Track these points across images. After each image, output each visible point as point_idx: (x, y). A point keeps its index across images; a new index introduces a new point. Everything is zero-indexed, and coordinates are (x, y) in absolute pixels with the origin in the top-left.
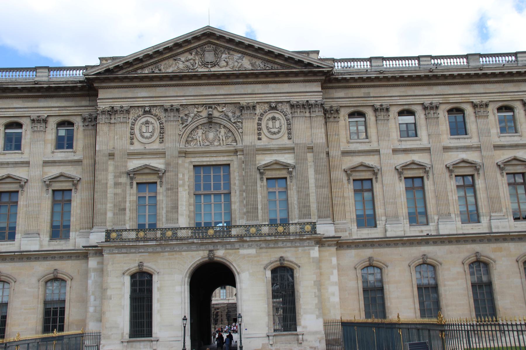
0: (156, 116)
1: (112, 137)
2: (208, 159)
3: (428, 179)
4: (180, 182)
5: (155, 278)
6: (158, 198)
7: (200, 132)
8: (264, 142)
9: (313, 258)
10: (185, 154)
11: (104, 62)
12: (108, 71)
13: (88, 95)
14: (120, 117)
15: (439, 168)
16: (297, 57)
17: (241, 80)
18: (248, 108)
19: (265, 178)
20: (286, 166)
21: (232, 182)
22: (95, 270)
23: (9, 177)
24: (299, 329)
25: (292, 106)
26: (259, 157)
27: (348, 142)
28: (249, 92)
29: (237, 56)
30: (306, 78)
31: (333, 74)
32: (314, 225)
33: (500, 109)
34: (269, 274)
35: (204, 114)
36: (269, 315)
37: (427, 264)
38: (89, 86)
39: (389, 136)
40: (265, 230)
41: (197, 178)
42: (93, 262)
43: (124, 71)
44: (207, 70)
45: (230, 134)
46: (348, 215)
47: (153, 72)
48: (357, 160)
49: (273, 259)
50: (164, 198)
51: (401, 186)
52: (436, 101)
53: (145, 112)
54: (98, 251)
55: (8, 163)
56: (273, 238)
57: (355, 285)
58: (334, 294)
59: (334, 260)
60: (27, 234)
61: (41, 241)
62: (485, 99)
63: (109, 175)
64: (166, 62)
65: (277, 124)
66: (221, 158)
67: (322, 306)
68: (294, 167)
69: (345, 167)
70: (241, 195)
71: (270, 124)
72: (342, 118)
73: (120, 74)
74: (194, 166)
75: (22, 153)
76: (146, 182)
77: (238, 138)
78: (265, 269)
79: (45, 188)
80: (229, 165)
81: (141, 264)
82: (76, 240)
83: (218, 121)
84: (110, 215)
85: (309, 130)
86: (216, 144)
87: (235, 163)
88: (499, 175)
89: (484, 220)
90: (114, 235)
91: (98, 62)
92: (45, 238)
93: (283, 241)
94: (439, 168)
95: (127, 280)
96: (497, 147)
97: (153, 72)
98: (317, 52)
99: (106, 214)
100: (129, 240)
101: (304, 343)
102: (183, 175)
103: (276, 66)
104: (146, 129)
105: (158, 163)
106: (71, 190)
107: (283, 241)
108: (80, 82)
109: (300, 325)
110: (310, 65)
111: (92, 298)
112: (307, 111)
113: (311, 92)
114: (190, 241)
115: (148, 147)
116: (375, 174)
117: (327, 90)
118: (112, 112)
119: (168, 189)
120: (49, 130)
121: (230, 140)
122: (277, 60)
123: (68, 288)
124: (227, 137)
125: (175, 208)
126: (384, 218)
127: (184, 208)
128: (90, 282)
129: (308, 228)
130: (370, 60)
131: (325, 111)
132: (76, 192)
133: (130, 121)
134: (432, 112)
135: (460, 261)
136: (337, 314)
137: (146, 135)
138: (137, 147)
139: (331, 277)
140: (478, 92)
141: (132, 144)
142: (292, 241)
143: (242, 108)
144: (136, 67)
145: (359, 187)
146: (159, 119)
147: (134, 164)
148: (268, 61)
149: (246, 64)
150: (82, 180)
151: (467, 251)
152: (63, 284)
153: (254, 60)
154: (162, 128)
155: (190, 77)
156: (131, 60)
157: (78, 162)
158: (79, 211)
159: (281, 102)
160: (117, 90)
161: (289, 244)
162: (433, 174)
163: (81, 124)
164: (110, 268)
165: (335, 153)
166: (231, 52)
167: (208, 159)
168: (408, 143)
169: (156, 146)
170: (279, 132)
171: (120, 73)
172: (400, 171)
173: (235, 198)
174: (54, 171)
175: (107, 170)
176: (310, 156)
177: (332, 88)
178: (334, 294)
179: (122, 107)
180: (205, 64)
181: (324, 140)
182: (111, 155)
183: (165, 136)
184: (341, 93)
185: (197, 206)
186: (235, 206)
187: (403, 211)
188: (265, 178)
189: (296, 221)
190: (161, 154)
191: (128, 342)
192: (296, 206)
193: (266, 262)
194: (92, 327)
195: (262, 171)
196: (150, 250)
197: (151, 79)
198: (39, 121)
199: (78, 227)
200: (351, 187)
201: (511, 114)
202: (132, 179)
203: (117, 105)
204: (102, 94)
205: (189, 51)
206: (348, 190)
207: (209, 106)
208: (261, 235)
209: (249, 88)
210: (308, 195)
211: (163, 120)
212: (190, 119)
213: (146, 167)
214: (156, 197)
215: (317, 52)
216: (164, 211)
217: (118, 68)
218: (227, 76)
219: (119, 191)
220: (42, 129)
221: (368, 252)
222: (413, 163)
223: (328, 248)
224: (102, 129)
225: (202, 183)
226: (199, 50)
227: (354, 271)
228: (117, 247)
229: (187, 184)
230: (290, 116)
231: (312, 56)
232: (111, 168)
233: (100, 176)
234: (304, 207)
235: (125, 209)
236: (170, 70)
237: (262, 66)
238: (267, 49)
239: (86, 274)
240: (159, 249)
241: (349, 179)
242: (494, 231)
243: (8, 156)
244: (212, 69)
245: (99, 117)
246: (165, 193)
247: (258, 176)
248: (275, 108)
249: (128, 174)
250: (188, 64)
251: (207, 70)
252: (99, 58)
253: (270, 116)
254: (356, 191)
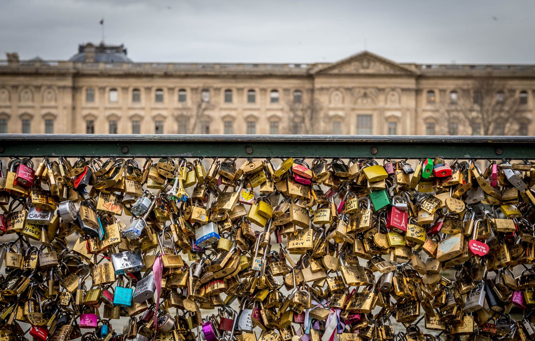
8: (388, 106)
10: (353, 110)
14: (325, 92)
16: (406, 67)
35: (362, 91)
87: (375, 114)
118: (322, 89)
138: (332, 105)
180: (363, 68)
205: (357, 61)
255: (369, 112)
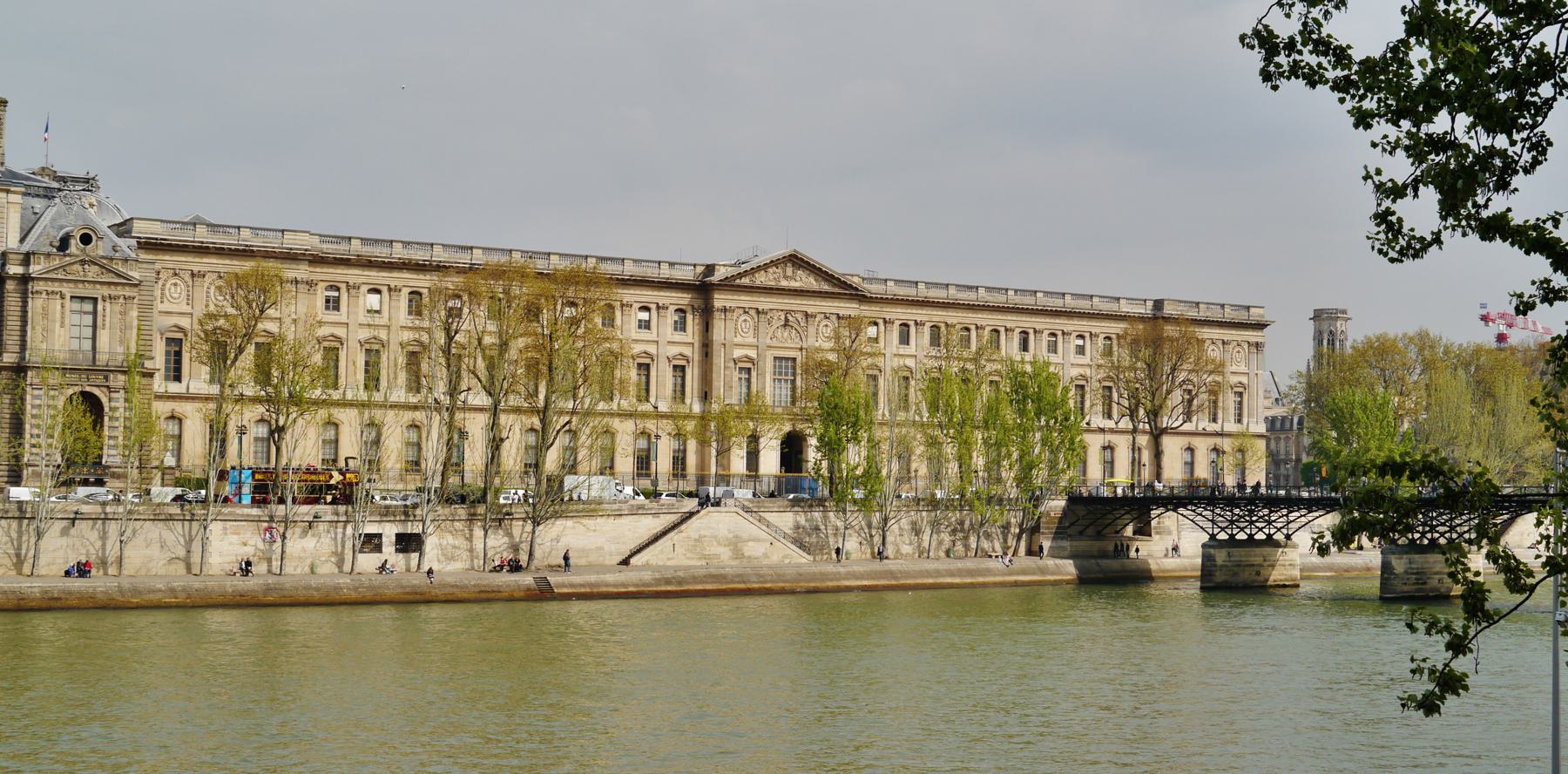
118: (725, 310)
147: (738, 353)
169: (751, 340)
180: (786, 277)
203: (728, 305)
207: (788, 312)
255: (791, 354)
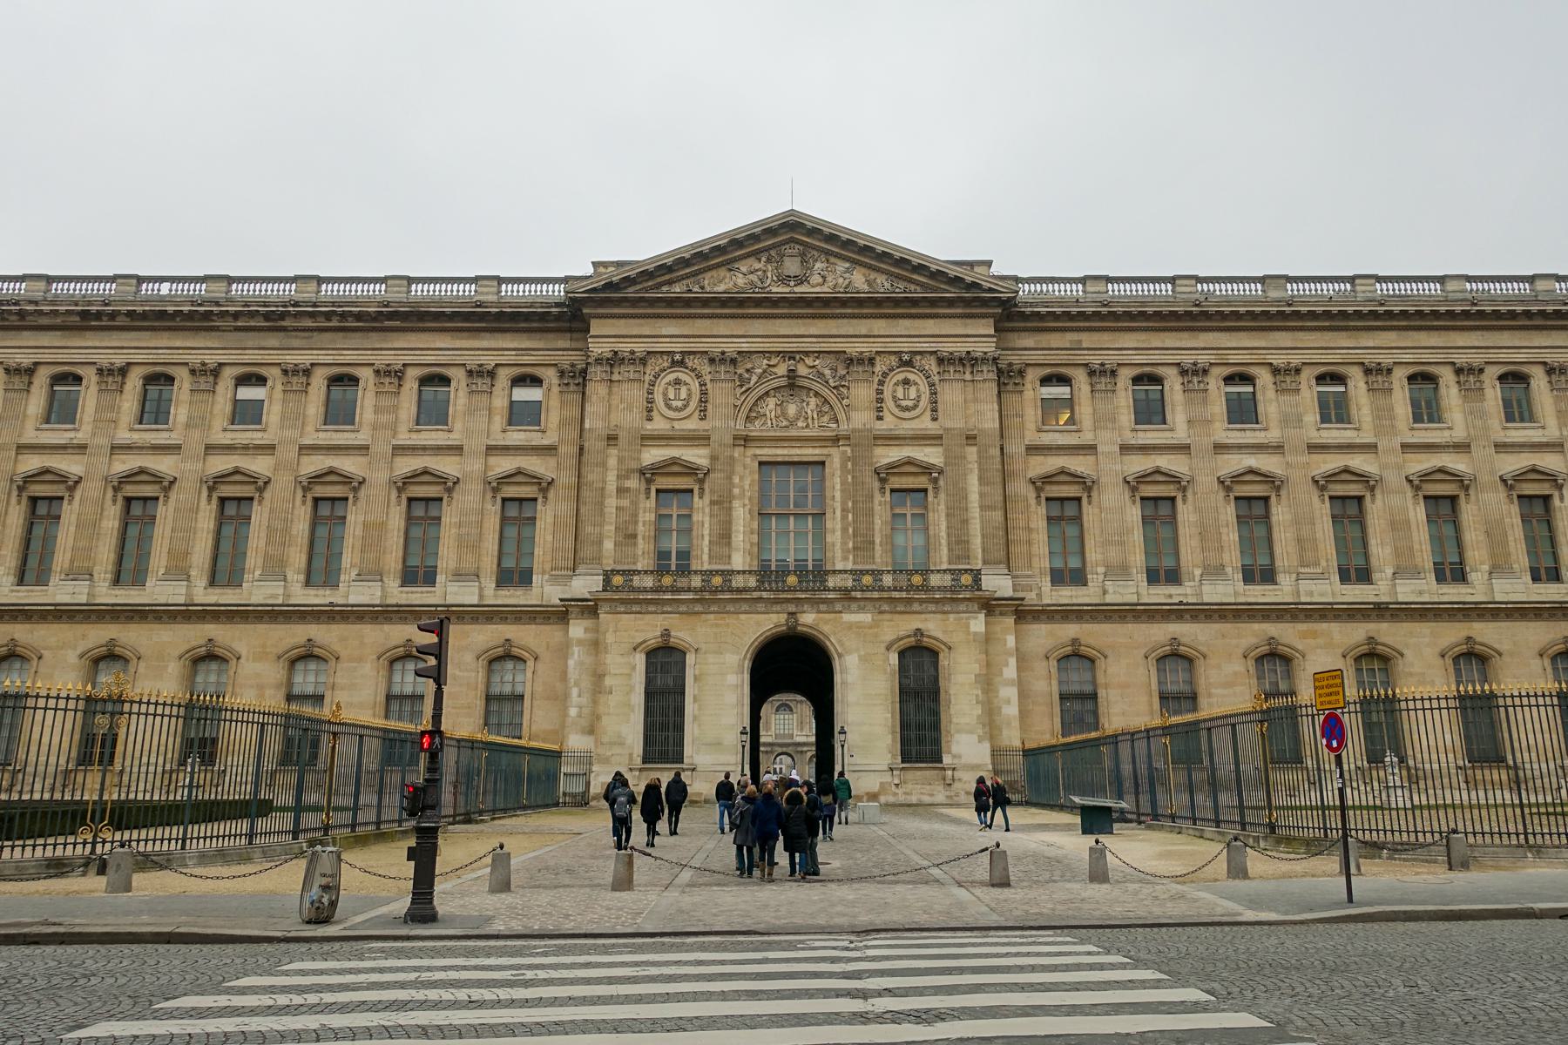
0: (693, 370)
1: (614, 405)
2: (785, 451)
3: (1184, 501)
4: (736, 491)
5: (690, 659)
6: (695, 518)
7: (772, 402)
8: (888, 424)
9: (975, 634)
10: (745, 441)
11: (602, 270)
12: (610, 286)
13: (570, 330)
14: (629, 371)
15: (1206, 483)
16: (953, 272)
17: (849, 311)
18: (860, 361)
19: (888, 488)
20: (926, 469)
21: (828, 494)
22: (580, 642)
23: (425, 472)
24: (947, 759)
25: (941, 361)
26: (879, 451)
27: (1039, 431)
28: (864, 332)
29: (842, 266)
30: (968, 311)
31: (1016, 305)
32: (977, 575)
33: (1321, 379)
34: (894, 659)
35: (782, 370)
36: (893, 732)
37: (1176, 657)
38: (573, 312)
39: (1114, 420)
40: (888, 580)
41: (763, 484)
42: (578, 629)
43: (638, 287)
44: (787, 290)
45: (826, 408)
46: (1035, 561)
47: (690, 291)
48: (1053, 463)
49: (902, 633)
50: (707, 519)
51: (1134, 513)
52: (1203, 359)
53: (674, 363)
54: (589, 608)
55: (424, 448)
56: (904, 595)
57: (1046, 684)
58: (1008, 702)
59: (1011, 641)
60: (459, 575)
61: (481, 589)
62: (1296, 359)
63: (609, 472)
64: (714, 273)
65: (913, 393)
66: (810, 451)
67: (990, 722)
68: (941, 472)
69: (1031, 474)
70: (844, 517)
71: (900, 393)
72: (1028, 386)
73: (631, 293)
74: (761, 463)
75: (450, 431)
76: (672, 485)
77: (841, 416)
78: (888, 649)
79: (489, 495)
80: (823, 463)
81: (666, 634)
82: (545, 591)
83: (806, 383)
84: (609, 545)
85: (970, 405)
86: (800, 424)
87: (835, 457)
88: (1316, 499)
89: (1285, 581)
90: (618, 580)
91: (590, 271)
92: (490, 584)
93: (921, 601)
94: (1206, 483)
95: (640, 660)
96: (1314, 448)
97: (690, 291)
98: (989, 264)
99: (601, 543)
100: (645, 590)
101: (956, 785)
102: (741, 478)
103: (913, 287)
104: (676, 393)
105: (697, 456)
106: (535, 500)
107: (921, 601)
108: (557, 305)
109: (949, 752)
110: (975, 286)
111: (575, 691)
112: (968, 370)
113: (977, 336)
114: (756, 595)
115: (677, 425)
116: (1089, 490)
117: (1003, 335)
118: (615, 360)
119: (712, 503)
120: (497, 390)
121: (826, 419)
122: (915, 277)
123: (529, 674)
124: (821, 413)
125: (724, 537)
126: (1101, 570)
127: (741, 537)
128: (571, 663)
129: (966, 579)
130: (1083, 280)
131: (1000, 372)
132: (545, 503)
133: (647, 378)
134: (1195, 380)
135: (1240, 652)
136: (1012, 738)
137: (674, 404)
138: (658, 425)
139: (1005, 670)
140: (1282, 346)
141: (650, 419)
142: (937, 601)
143: (850, 361)
144: (659, 280)
145: (1056, 513)
146: (698, 377)
148: (898, 277)
149: (859, 280)
150: (557, 483)
151: (1254, 634)
152: (520, 666)
153: (873, 275)
154: (704, 393)
155: (759, 303)
156: (651, 267)
157: (550, 450)
158: (549, 538)
159: (920, 353)
160: (623, 321)
161: (932, 607)
162: (1195, 494)
163: (555, 381)
164: (610, 638)
165: (1016, 448)
166: (832, 260)
167: (785, 451)
168: (1149, 435)
169: (692, 425)
170: (915, 406)
171: (631, 289)
172: (1134, 485)
173: (834, 523)
174: (505, 465)
175: (604, 465)
176: (972, 453)
177: (1013, 330)
178: (1008, 702)
179: (632, 353)
180: (784, 280)
181: (997, 425)
182: (612, 439)
183: (710, 407)
184: (1028, 341)
185: (763, 534)
186: (835, 537)
187: (1138, 560)
188: (888, 488)
189: (944, 567)
190: (699, 439)
191: (641, 770)
192: (944, 542)
193: (889, 636)
194: (576, 742)
195: (883, 475)
196: (683, 608)
197: (688, 303)
198: (480, 374)
199: (548, 566)
200: (1042, 510)
201: (1342, 389)
202: (649, 481)
203: (625, 347)
204: (596, 327)
205: (756, 254)
206: (1038, 517)
207: (790, 355)
208: (882, 589)
209: (862, 327)
210: (965, 522)
211: (708, 378)
212: (754, 379)
213: (674, 461)
214: (689, 516)
215: (989, 264)
216: (706, 542)
217: (629, 281)
218: (826, 302)
219: (625, 503)
220: (485, 388)
221: (1070, 630)
222: (1158, 471)
223: (1001, 619)
224: (596, 390)
225: (774, 494)
226: (773, 253)
227: (1045, 663)
228: (623, 601)
229: (748, 494)
230: (936, 379)
231: (976, 269)
232: (612, 462)
233: (591, 476)
234: (959, 542)
235: (634, 536)
236: (721, 288)
237: (887, 285)
238: (897, 255)
239: (563, 651)
240: (699, 608)
241: (1038, 497)
242: (1303, 600)
243: (423, 435)
244: (797, 289)
245: (591, 369)
246: (707, 510)
247: (877, 484)
248: (909, 364)
249: (642, 472)
250: (753, 277)
251: (787, 290)
252: (593, 263)
253: (901, 377)
254: (1049, 519)
